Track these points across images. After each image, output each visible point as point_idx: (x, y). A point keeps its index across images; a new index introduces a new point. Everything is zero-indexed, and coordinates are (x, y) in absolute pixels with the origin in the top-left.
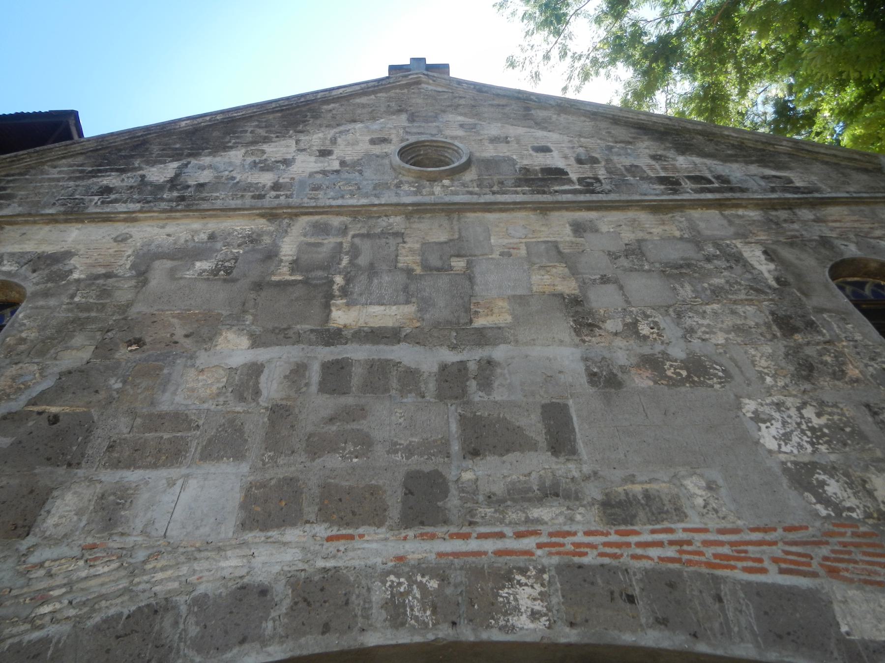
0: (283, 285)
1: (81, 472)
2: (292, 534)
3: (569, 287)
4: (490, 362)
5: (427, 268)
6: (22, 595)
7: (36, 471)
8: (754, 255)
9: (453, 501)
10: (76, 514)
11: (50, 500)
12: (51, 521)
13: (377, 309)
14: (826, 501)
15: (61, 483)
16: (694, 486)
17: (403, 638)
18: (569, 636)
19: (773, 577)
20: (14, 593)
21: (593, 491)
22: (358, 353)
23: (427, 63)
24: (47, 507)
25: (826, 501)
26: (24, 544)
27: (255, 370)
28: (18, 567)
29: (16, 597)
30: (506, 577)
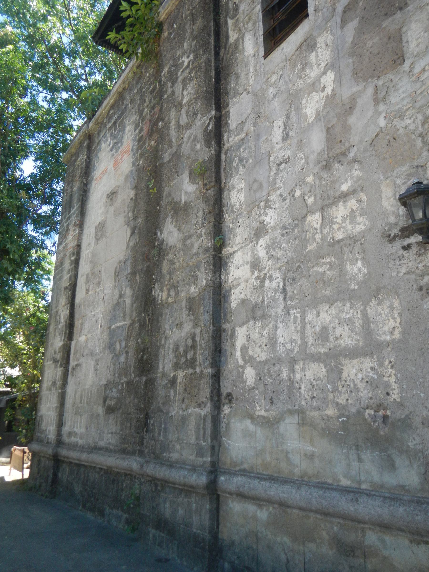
1: (411, 8)
6: (424, 90)
7: (384, 26)
10: (425, 32)
11: (403, 35)
12: (412, 46)
15: (404, 22)
20: (418, 93)
24: (404, 40)
26: (406, 66)
28: (411, 79)
29: (421, 93)
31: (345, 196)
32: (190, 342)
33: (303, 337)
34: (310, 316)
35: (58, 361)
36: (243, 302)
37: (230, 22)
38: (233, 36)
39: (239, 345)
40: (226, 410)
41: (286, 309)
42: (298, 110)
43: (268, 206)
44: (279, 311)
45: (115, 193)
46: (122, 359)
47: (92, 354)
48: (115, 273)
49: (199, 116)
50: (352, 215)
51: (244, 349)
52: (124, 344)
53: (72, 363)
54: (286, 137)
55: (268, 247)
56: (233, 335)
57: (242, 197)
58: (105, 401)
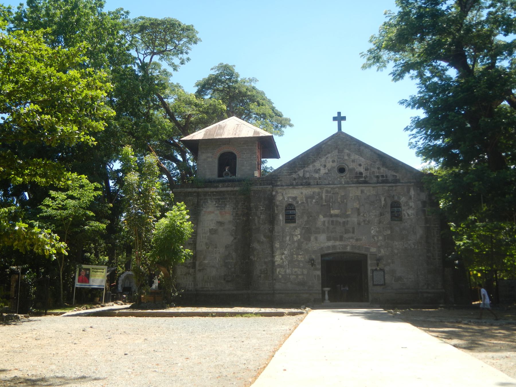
0: (324, 205)
2: (331, 242)
3: (358, 206)
4: (348, 221)
5: (341, 202)
8: (383, 199)
9: (344, 239)
13: (336, 211)
14: (374, 239)
16: (364, 238)
17: (340, 251)
18: (351, 251)
19: (367, 246)
21: (355, 238)
22: (334, 219)
23: (342, 116)
25: (374, 239)
27: (324, 222)
30: (347, 246)
31: (301, 255)
32: (265, 270)
33: (292, 272)
34: (293, 269)
35: (190, 267)
36: (278, 265)
37: (275, 208)
38: (276, 212)
39: (277, 271)
40: (274, 281)
41: (289, 267)
42: (293, 237)
43: (285, 250)
44: (287, 267)
45: (223, 223)
46: (233, 270)
47: (213, 267)
48: (226, 247)
49: (267, 224)
50: (301, 258)
51: (279, 272)
52: (233, 266)
53: (197, 267)
54: (289, 240)
55: (285, 257)
56: (276, 270)
57: (278, 246)
58: (225, 279)
